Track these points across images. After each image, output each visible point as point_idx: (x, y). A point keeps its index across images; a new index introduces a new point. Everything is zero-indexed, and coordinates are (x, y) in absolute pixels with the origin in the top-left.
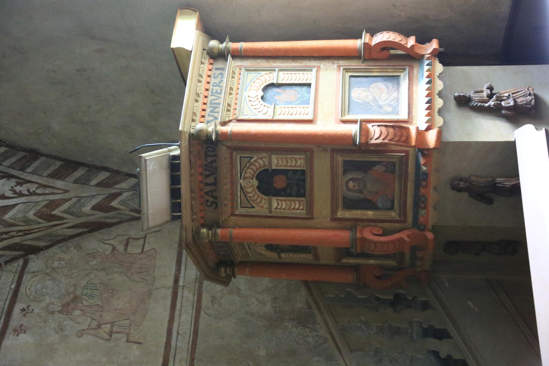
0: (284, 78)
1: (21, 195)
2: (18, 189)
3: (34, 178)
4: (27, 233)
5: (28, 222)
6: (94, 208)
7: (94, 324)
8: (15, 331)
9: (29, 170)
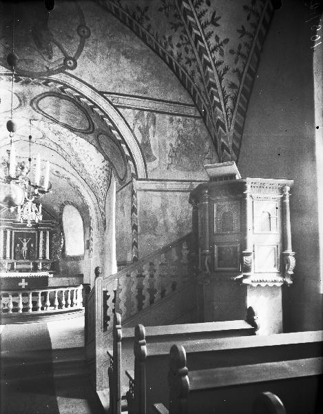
0: (273, 220)
1: (226, 112)
3: (234, 116)
4: (211, 117)
5: (216, 116)
6: (223, 143)
7: (175, 150)
9: (239, 114)
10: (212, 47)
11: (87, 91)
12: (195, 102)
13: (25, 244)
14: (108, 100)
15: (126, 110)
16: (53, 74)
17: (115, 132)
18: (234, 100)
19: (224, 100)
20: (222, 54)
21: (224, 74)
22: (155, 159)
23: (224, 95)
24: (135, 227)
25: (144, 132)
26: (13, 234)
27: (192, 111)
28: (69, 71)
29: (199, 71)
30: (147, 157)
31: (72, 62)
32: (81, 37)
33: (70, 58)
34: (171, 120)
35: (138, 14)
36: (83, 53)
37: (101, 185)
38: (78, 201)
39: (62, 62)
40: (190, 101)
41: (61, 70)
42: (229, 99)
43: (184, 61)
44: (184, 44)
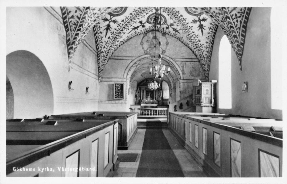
0: (209, 91)
10: (199, 46)
11: (168, 58)
13: (149, 95)
18: (207, 58)
20: (202, 47)
22: (185, 74)
24: (180, 92)
25: (183, 67)
27: (195, 60)
28: (164, 54)
30: (184, 74)
32: (166, 45)
34: (190, 63)
35: (181, 38)
38: (167, 80)
40: (196, 58)
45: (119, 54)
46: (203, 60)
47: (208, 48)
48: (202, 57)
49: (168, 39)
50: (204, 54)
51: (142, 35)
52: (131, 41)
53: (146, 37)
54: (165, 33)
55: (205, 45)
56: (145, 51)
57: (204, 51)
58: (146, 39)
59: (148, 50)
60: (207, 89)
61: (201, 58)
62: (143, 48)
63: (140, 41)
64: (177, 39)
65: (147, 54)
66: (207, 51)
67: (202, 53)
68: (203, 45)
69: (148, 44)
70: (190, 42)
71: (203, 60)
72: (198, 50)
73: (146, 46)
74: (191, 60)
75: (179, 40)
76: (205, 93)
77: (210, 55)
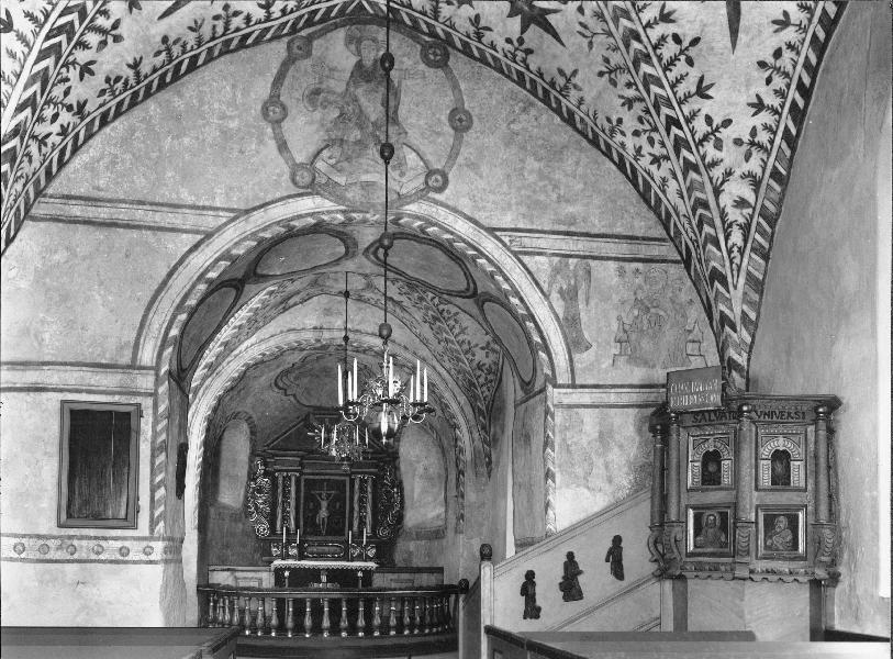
1: (730, 252)
2: (735, 249)
4: (700, 261)
5: (707, 261)
8: (622, 267)
11: (463, 228)
12: (669, 234)
14: (505, 245)
15: (537, 258)
16: (408, 204)
17: (514, 301)
18: (746, 229)
19: (725, 231)
20: (719, 145)
21: (722, 184)
23: (723, 222)
26: (343, 478)
27: (667, 250)
29: (675, 177)
30: (575, 344)
31: (439, 178)
33: (437, 171)
36: (460, 159)
37: (482, 380)
39: (422, 179)
40: (659, 232)
41: (421, 195)
42: (735, 228)
43: (645, 162)
44: (645, 131)
45: (102, 183)
46: (717, 244)
47: (760, 146)
48: (713, 226)
49: (463, 86)
50: (725, 200)
51: (279, 50)
52: (191, 86)
53: (305, 64)
54: (449, 41)
55: (743, 125)
56: (295, 168)
57: (729, 173)
58: (310, 82)
59: (320, 165)
60: (781, 444)
61: (707, 229)
62: (283, 146)
63: (263, 89)
64: (533, 92)
65: (312, 188)
66: (749, 175)
67: (717, 192)
68: (727, 123)
69: (317, 115)
70: (629, 103)
71: (717, 244)
72: (689, 166)
73: (304, 130)
74: (623, 249)
75: (546, 100)
76: (766, 479)
77: (772, 208)
